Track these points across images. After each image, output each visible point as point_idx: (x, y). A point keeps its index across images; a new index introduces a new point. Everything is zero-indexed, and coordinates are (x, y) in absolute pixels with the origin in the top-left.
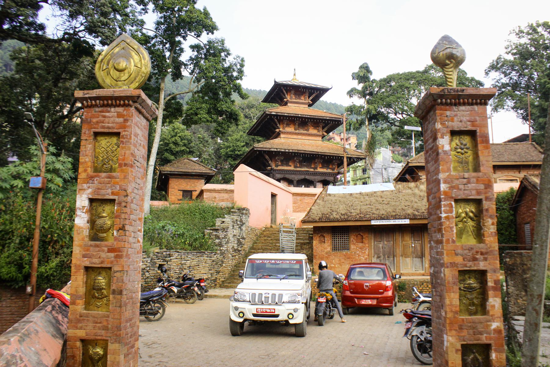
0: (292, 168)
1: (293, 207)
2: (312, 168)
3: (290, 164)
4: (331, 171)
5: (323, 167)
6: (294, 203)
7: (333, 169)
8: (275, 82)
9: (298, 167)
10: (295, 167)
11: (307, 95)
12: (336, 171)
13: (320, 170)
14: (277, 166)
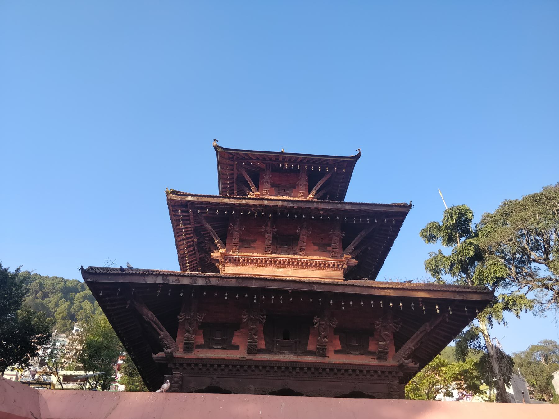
0: (241, 354)
2: (312, 353)
3: (236, 340)
4: (375, 362)
5: (345, 350)
7: (382, 355)
9: (261, 351)
10: (252, 349)
11: (303, 181)
12: (391, 362)
14: (188, 347)
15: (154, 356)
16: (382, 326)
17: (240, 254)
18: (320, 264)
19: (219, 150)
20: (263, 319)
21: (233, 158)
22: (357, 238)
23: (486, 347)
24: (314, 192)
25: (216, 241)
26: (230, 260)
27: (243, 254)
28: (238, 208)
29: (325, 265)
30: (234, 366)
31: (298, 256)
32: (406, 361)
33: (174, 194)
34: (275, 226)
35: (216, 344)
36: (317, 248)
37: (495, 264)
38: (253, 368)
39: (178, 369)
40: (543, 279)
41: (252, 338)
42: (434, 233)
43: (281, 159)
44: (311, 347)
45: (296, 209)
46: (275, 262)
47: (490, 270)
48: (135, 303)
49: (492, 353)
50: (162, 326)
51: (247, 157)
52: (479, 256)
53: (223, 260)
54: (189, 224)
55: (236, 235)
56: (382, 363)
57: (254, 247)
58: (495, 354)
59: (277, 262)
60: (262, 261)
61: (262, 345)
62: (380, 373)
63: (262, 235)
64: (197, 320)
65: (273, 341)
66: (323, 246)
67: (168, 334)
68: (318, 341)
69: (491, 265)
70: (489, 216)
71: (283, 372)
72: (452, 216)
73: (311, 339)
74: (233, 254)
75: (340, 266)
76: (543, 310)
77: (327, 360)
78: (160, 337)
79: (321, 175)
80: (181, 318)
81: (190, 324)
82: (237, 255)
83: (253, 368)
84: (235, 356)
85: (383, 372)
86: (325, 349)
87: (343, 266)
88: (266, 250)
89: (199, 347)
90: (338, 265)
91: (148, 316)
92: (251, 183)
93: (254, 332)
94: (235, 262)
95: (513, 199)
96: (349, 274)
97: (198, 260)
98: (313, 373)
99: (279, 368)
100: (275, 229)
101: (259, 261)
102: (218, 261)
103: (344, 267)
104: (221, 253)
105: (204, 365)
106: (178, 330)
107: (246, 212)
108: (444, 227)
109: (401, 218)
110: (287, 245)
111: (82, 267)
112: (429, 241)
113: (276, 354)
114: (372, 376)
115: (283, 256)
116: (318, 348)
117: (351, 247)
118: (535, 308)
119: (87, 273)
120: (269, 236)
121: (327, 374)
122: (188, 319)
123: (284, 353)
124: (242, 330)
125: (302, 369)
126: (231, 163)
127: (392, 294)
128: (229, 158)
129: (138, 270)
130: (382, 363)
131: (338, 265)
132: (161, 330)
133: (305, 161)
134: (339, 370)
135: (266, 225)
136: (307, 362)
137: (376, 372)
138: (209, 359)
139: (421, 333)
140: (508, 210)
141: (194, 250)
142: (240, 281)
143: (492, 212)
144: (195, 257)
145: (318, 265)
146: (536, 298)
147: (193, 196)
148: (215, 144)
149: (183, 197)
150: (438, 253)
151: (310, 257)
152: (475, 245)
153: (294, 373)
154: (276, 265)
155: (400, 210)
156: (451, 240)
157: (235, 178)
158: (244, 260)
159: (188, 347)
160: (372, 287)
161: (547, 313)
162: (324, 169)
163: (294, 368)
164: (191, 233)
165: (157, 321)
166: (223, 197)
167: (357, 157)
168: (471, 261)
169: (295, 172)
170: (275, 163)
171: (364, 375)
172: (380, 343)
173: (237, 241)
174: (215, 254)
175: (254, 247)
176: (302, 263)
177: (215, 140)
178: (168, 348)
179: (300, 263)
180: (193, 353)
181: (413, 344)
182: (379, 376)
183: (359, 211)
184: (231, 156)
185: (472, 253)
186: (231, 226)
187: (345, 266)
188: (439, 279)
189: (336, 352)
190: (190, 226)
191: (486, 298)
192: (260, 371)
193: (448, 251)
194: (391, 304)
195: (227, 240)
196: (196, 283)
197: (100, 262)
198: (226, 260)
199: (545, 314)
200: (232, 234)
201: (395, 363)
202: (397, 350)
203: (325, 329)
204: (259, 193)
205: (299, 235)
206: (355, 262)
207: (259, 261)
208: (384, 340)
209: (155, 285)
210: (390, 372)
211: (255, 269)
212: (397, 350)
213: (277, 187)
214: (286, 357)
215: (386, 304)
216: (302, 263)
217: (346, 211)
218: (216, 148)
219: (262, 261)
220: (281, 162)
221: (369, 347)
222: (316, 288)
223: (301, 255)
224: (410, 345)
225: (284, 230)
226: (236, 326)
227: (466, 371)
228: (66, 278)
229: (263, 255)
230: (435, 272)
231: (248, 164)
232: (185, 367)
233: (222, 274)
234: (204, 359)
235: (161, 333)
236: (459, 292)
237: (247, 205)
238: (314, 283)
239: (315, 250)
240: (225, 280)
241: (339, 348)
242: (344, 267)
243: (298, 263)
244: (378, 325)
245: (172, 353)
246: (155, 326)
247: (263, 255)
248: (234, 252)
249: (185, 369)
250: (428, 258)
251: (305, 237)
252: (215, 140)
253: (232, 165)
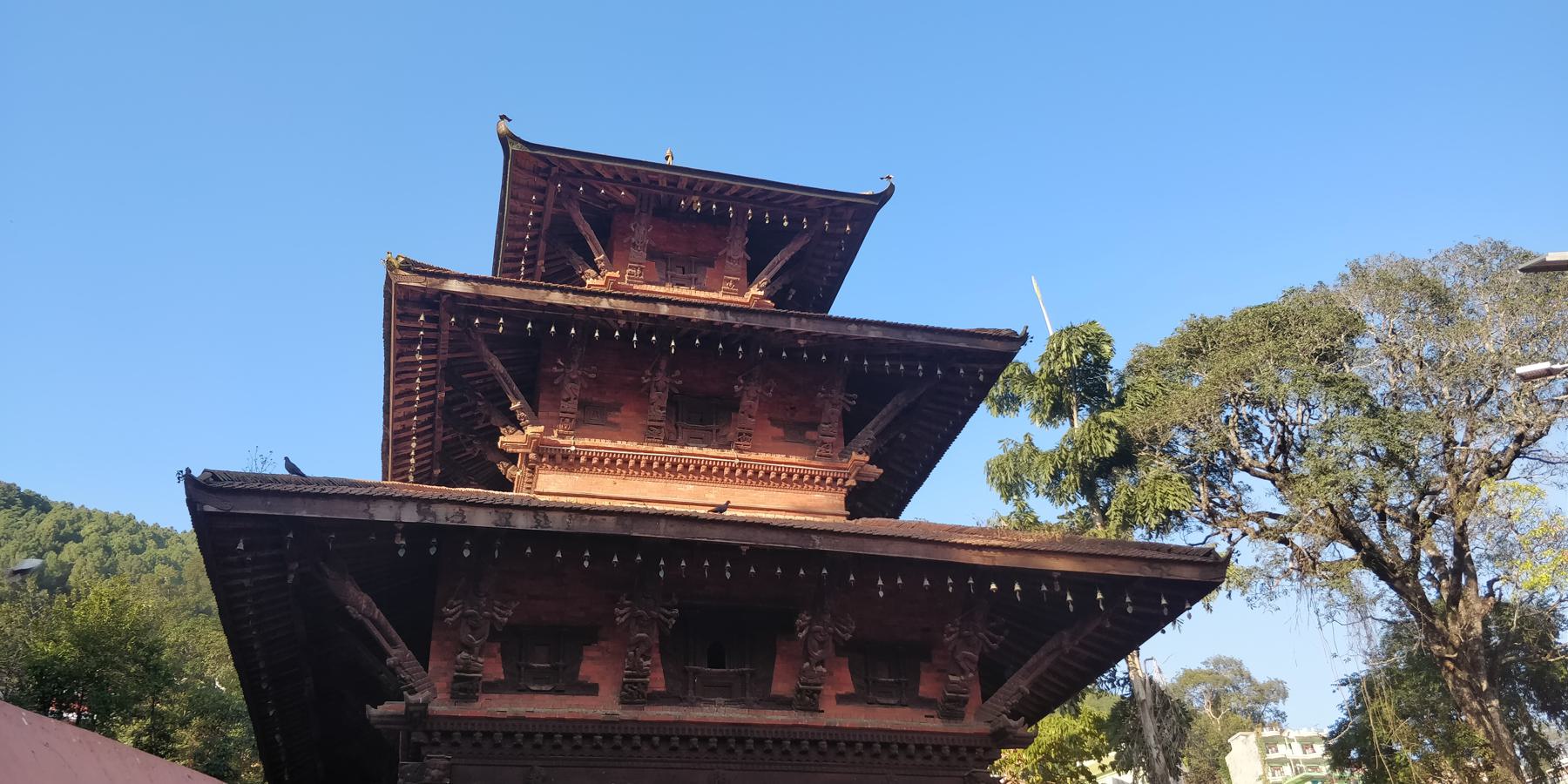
0: (602, 706)
3: (589, 670)
4: (936, 725)
5: (865, 694)
7: (952, 708)
10: (633, 694)
11: (737, 250)
12: (973, 724)
13: (838, 716)
14: (465, 689)
15: (374, 712)
16: (960, 637)
17: (580, 442)
18: (790, 475)
19: (513, 147)
20: (669, 617)
21: (548, 171)
22: (884, 411)
23: (1127, 681)
24: (763, 280)
25: (515, 405)
26: (552, 457)
27: (587, 442)
28: (581, 317)
29: (801, 476)
30: (588, 737)
31: (732, 453)
32: (1012, 722)
33: (407, 269)
34: (678, 373)
35: (537, 680)
36: (780, 432)
37: (1166, 477)
38: (637, 740)
39: (437, 744)
40: (1262, 514)
41: (636, 666)
42: (1017, 389)
43: (682, 185)
44: (780, 687)
45: (739, 330)
46: (674, 465)
47: (1154, 491)
48: (327, 570)
49: (1142, 696)
50: (394, 634)
51: (586, 172)
52: (1126, 456)
53: (532, 456)
54: (434, 352)
55: (571, 390)
56: (954, 727)
57: (616, 425)
58: (1150, 700)
59: (680, 467)
60: (638, 463)
61: (657, 682)
62: (947, 751)
63: (641, 394)
64: (493, 618)
65: (686, 672)
66: (796, 426)
67: (409, 654)
68: (803, 672)
69: (1157, 478)
70: (1149, 353)
71: (713, 750)
72: (1069, 352)
73: (779, 667)
74: (561, 441)
75: (840, 482)
76: (1272, 596)
77: (821, 720)
78: (390, 661)
79: (785, 237)
80: (451, 612)
81: (473, 629)
82: (571, 443)
83: (637, 740)
84: (590, 712)
85: (954, 749)
86: (819, 692)
87: (845, 480)
88: (649, 435)
89: (492, 687)
90: (835, 480)
91: (358, 607)
92: (594, 244)
93: (642, 649)
94: (566, 461)
95: (1211, 315)
96: (862, 500)
97: (438, 447)
98: (786, 753)
99: (704, 740)
100: (678, 378)
101: (631, 463)
102: (512, 458)
103: (848, 483)
104: (529, 439)
105: (509, 735)
106: (433, 643)
107: (607, 333)
108: (1044, 376)
109: (996, 367)
110: (701, 422)
111: (188, 470)
112: (1000, 411)
113: (692, 705)
114: (929, 758)
115: (695, 450)
116: (799, 691)
117: (867, 434)
118: (1255, 589)
119: (203, 490)
120: (659, 398)
121: (822, 753)
122: (471, 615)
123: (713, 703)
124: (603, 644)
125: (759, 742)
126: (543, 183)
127: (1000, 560)
128: (536, 171)
129: (330, 481)
130: (954, 727)
131: (835, 480)
132: (393, 644)
133: (746, 196)
134: (851, 744)
135: (656, 369)
136: (772, 726)
137: (937, 748)
138: (524, 718)
139: (1049, 654)
140: (1198, 343)
141: (431, 420)
142: (628, 522)
143: (1156, 344)
144: (431, 439)
145: (784, 476)
146: (1259, 565)
147: (464, 278)
148: (502, 128)
149: (434, 280)
150: (1021, 441)
151: (762, 456)
152: (1121, 429)
153: (739, 751)
154: (676, 474)
155: (999, 346)
156: (1059, 410)
157: (546, 224)
158: (589, 459)
159: (465, 689)
160: (955, 545)
161: (1280, 601)
163: (741, 741)
164: (434, 377)
165: (383, 619)
166: (547, 288)
167: (883, 198)
168: (1106, 468)
169: (717, 223)
170: (662, 193)
171: (911, 757)
172: (952, 678)
173: (572, 406)
174: (509, 439)
176: (745, 471)
177: (503, 117)
178: (413, 691)
179: (738, 472)
180: (477, 705)
181: (1027, 682)
182: (945, 758)
183: (898, 344)
184: (542, 165)
185: (1111, 448)
186: (559, 366)
187: (851, 482)
188: (1024, 511)
189: (842, 699)
190: (433, 357)
191: (1210, 575)
192: (654, 747)
193: (1050, 438)
194: (993, 586)
195: (542, 402)
196: (508, 523)
197: (234, 459)
198: (541, 456)
199: (1276, 603)
200: (560, 388)
201: (986, 728)
202: (985, 698)
203: (822, 644)
204: (617, 274)
205: (739, 399)
206: (876, 471)
207: (631, 463)
208: (963, 672)
209: (389, 528)
210: (971, 750)
211: (620, 482)
212: (985, 698)
213: (665, 259)
214: (719, 713)
215: (1006, 587)
216: (745, 471)
217: (864, 341)
218: (506, 139)
219: (638, 463)
220: (681, 191)
221: (921, 688)
222: (819, 544)
223: (741, 451)
224: (1019, 684)
226: (586, 635)
227: (1075, 739)
229: (643, 447)
230: (1011, 489)
231: (592, 191)
232: (457, 739)
233: (518, 494)
234: (509, 718)
235: (393, 652)
236: (1151, 562)
237: (609, 313)
238: (816, 531)
239: (774, 439)
240: (588, 517)
241: (851, 689)
242: (848, 483)
243: (733, 470)
244: (950, 634)
245: (425, 704)
246: (376, 632)
247: (643, 447)
248: (561, 436)
249: (456, 744)
250: (996, 452)
251: (756, 405)
252: (503, 117)
253: (543, 191)
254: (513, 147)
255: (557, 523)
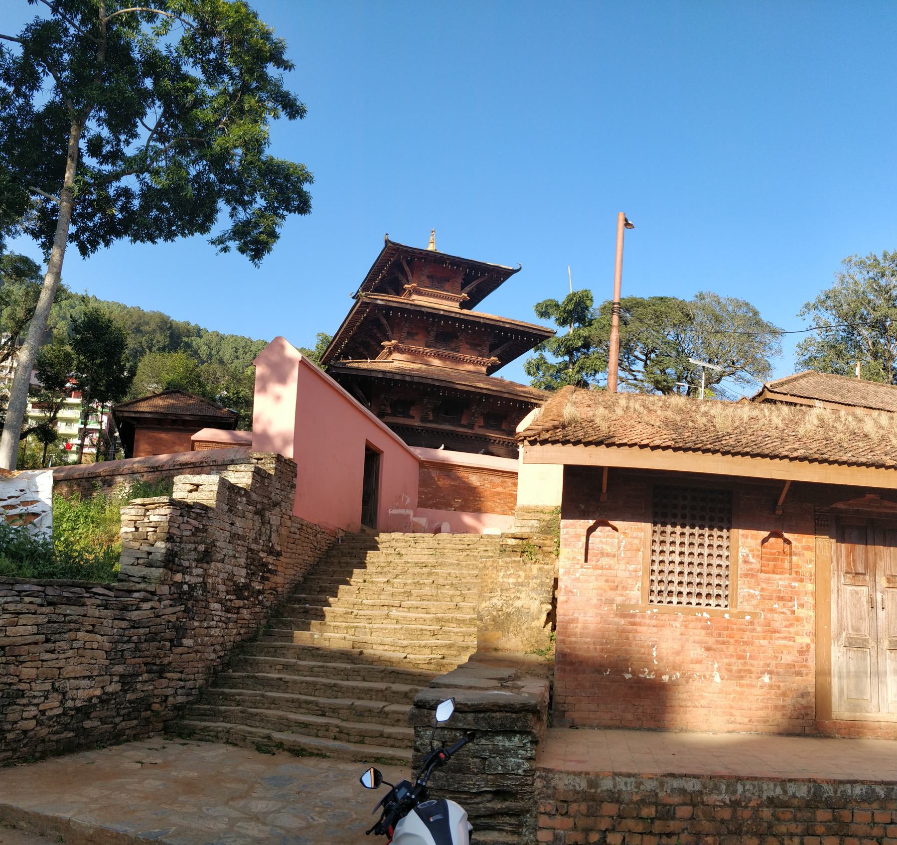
1: (420, 493)
6: (420, 486)
8: (387, 241)
19: (389, 244)
55: (406, 330)
120: (433, 334)
162: (476, 273)
175: (416, 340)
188: (542, 357)
225: (445, 332)
228: (221, 333)
254: (389, 244)
255: (416, 380)
